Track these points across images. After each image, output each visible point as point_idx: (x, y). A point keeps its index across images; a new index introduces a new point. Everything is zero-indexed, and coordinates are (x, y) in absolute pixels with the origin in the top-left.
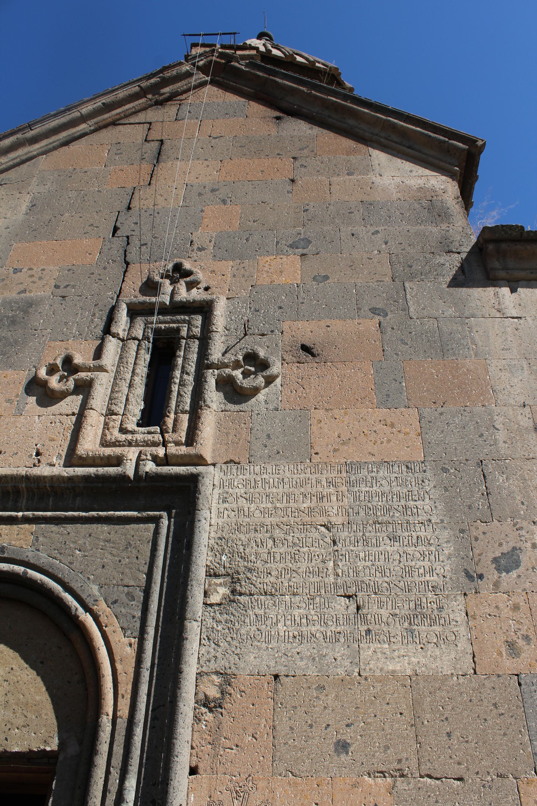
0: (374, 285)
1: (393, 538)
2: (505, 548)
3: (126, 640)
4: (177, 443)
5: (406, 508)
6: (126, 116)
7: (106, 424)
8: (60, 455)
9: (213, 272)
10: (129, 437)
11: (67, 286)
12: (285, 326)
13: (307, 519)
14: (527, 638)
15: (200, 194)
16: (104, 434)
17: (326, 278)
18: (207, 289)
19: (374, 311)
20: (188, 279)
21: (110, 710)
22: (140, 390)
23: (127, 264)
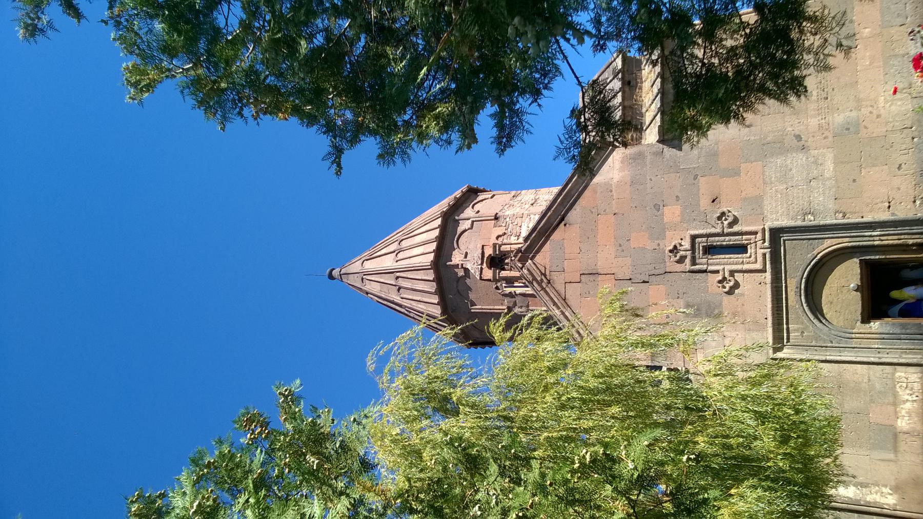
0: (681, 180)
1: (791, 170)
2: (794, 138)
3: (826, 243)
4: (756, 238)
5: (780, 167)
6: (560, 295)
7: (747, 263)
8: (761, 276)
9: (672, 239)
10: (753, 254)
11: (678, 294)
12: (702, 209)
13: (784, 195)
14: (823, 134)
15: (623, 251)
16: (752, 263)
17: (677, 197)
18: (682, 239)
19: (695, 177)
20: (678, 246)
21: (847, 244)
22: (732, 256)
23: (666, 272)
